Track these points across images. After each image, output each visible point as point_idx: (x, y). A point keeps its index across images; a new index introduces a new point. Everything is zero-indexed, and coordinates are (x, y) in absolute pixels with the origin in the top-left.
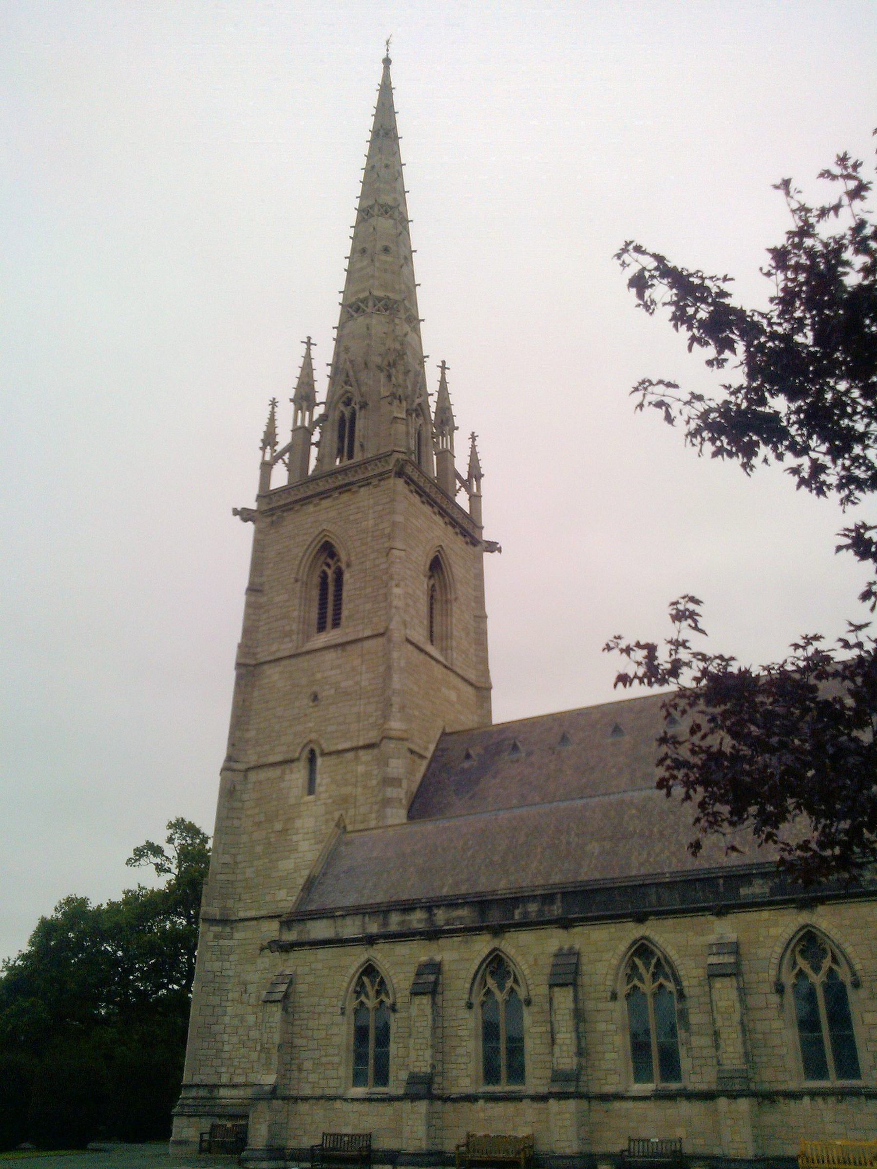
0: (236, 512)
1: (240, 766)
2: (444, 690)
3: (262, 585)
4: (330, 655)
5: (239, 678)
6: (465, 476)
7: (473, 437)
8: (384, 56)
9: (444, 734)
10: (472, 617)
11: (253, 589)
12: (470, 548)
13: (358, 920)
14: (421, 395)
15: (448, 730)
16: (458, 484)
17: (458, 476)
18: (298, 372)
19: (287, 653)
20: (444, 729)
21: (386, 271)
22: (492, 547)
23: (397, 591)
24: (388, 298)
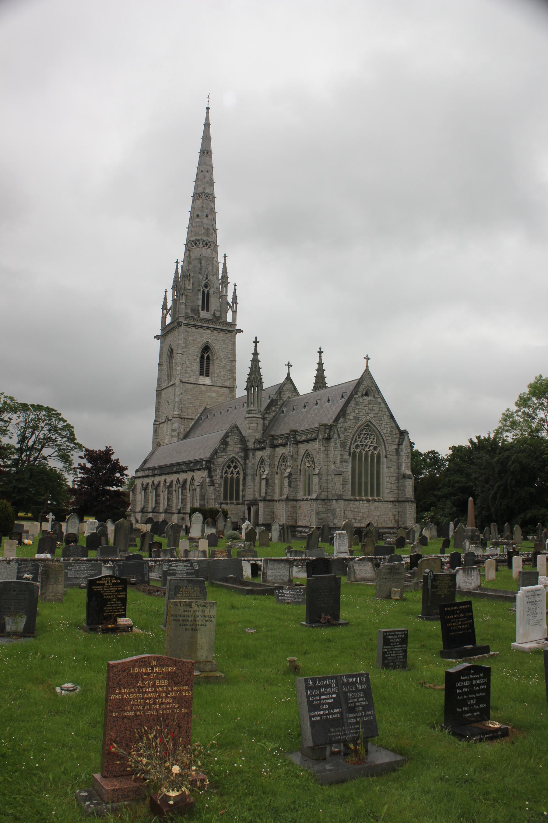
0: (155, 337)
1: (158, 423)
2: (207, 394)
3: (162, 362)
4: (170, 388)
5: (157, 395)
6: (231, 304)
7: (235, 285)
8: (207, 106)
9: (206, 409)
10: (229, 361)
11: (160, 365)
12: (229, 335)
13: (141, 472)
14: (207, 278)
15: (208, 407)
16: (228, 307)
17: (228, 303)
18: (173, 276)
19: (165, 387)
20: (206, 407)
21: (196, 227)
22: (240, 331)
23: (178, 368)
24: (196, 239)
